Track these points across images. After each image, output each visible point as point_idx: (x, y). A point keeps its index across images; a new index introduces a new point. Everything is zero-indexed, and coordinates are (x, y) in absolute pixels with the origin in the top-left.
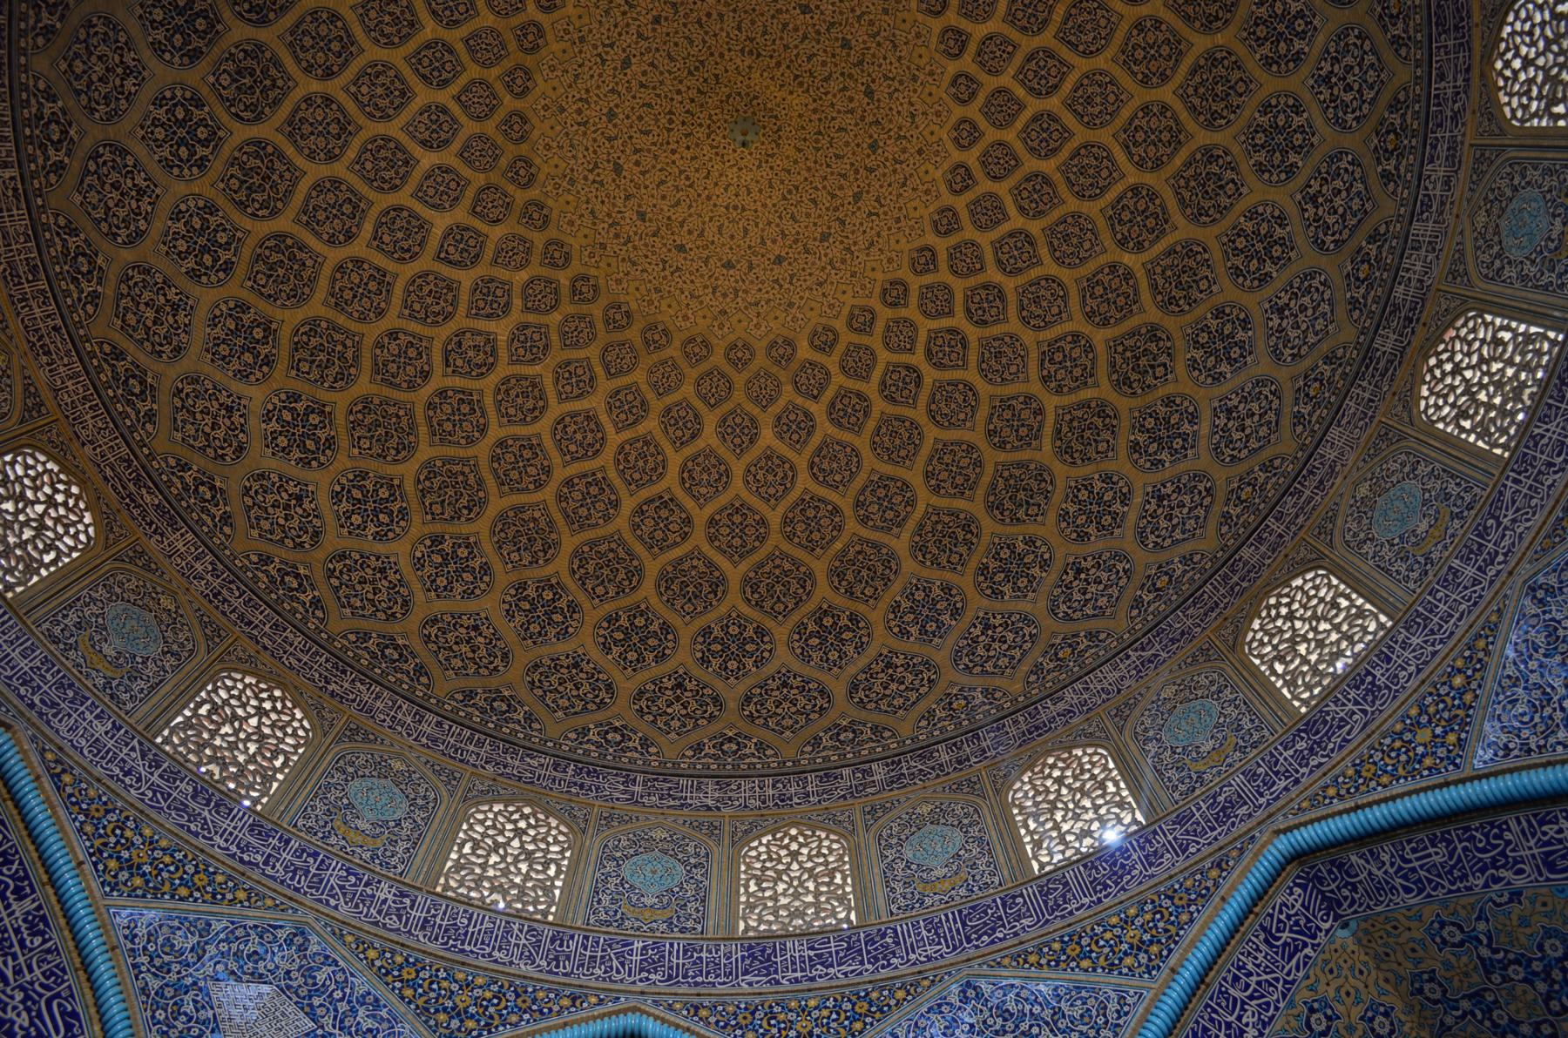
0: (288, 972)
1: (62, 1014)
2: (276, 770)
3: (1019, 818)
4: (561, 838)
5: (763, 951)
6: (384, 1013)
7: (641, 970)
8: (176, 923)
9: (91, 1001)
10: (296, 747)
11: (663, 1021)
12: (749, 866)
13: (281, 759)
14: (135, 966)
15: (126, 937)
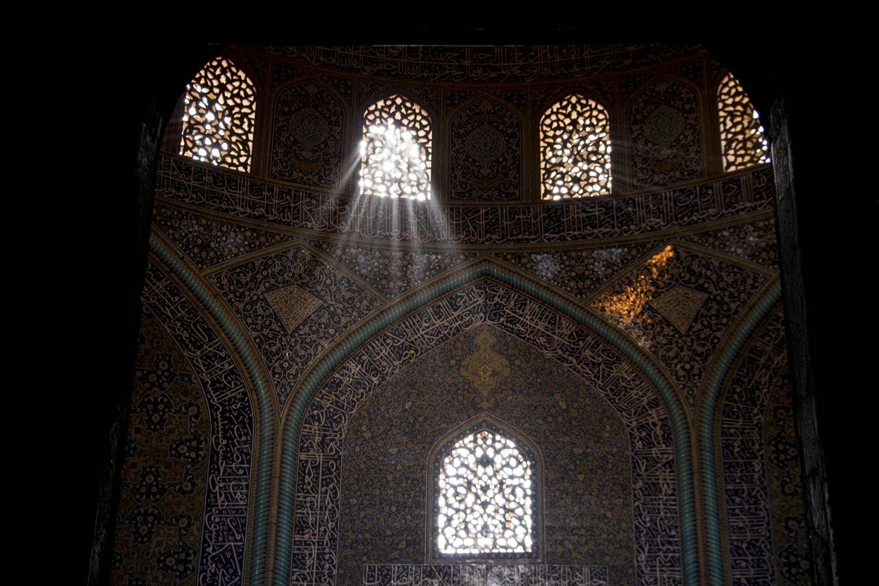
0: (300, 275)
1: (204, 329)
2: (246, 133)
3: (722, 114)
4: (424, 122)
5: (556, 212)
6: (354, 288)
7: (487, 232)
8: (238, 270)
9: (215, 323)
10: (250, 107)
11: (502, 267)
12: (546, 137)
13: (245, 120)
14: (229, 301)
15: (219, 288)
